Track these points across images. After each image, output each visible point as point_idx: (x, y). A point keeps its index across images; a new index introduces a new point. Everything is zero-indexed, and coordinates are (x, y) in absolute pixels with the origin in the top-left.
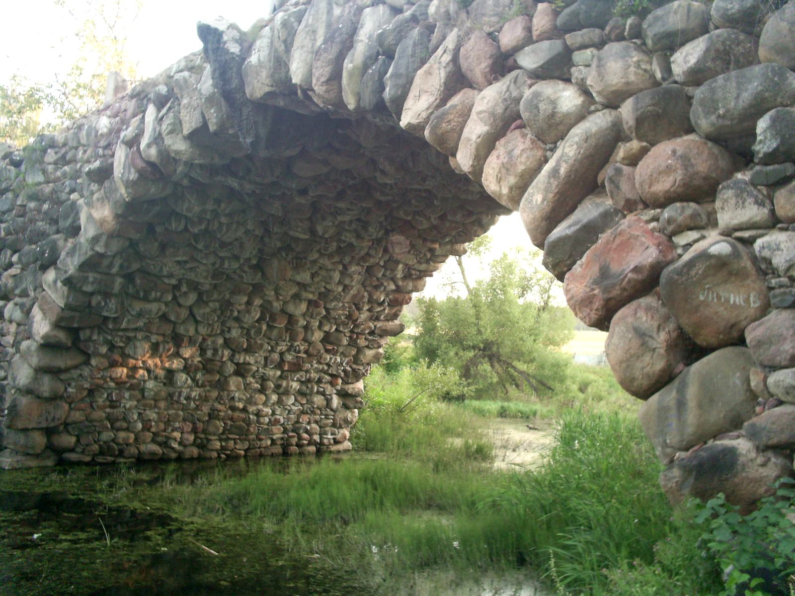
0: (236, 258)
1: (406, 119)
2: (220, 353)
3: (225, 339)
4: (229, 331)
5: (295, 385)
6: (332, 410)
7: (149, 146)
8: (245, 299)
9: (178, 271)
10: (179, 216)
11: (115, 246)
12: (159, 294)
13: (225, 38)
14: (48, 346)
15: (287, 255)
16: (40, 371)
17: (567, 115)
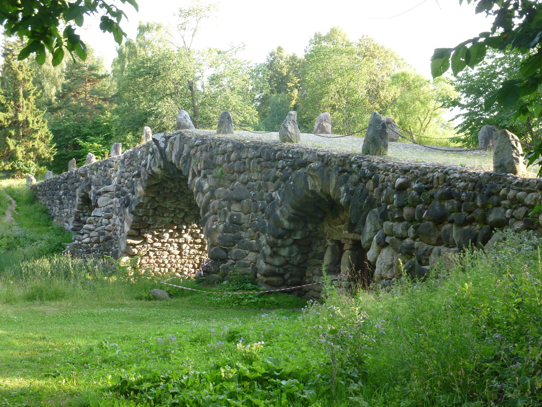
7: (148, 169)
9: (172, 205)
10: (167, 188)
11: (146, 200)
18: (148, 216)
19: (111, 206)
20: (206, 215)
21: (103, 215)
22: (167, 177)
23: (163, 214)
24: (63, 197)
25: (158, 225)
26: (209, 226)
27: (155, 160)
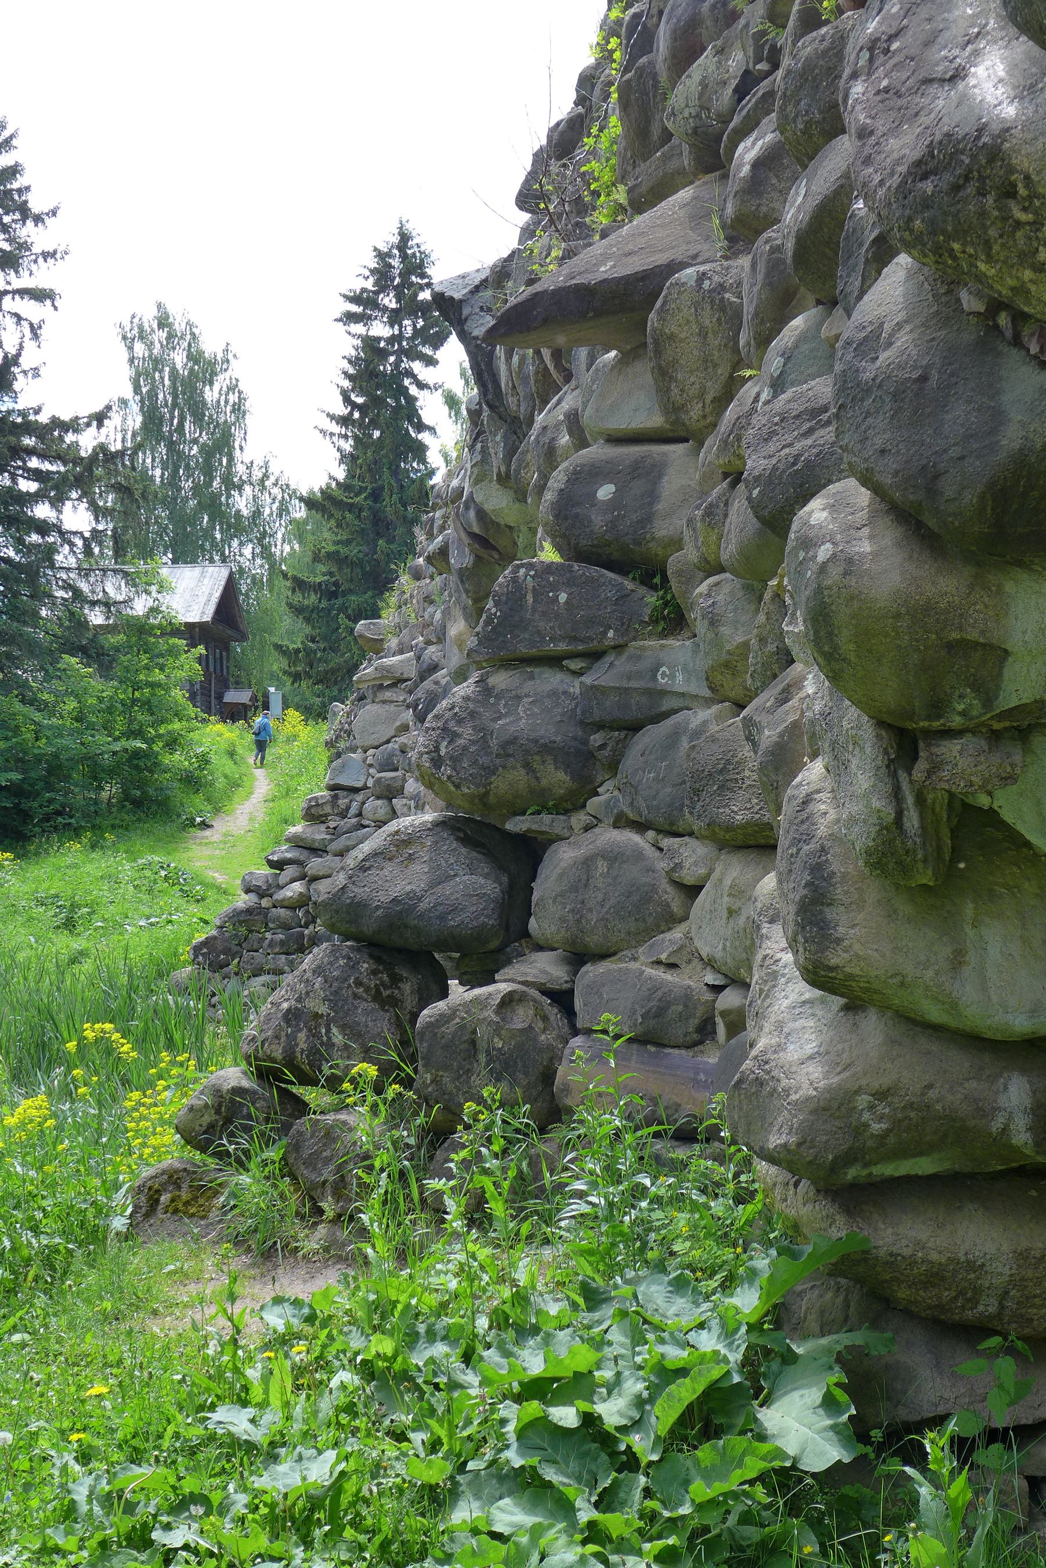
13: (466, 312)
19: (402, 740)
21: (370, 783)
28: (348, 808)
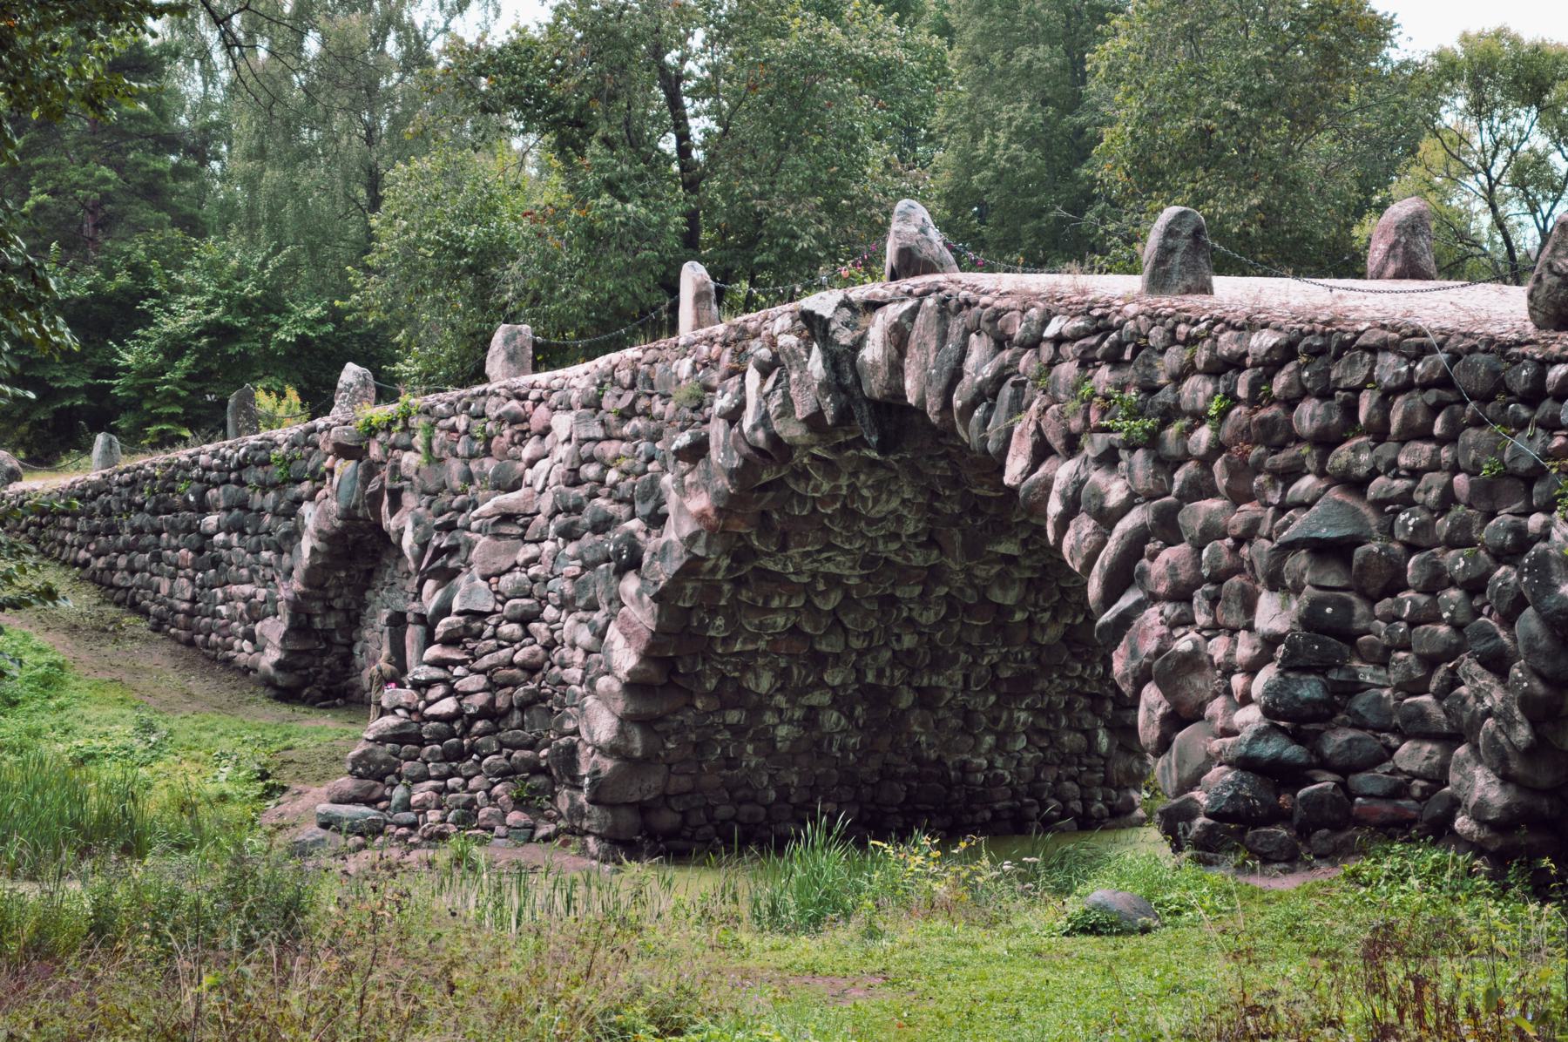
0: (895, 536)
1: (1008, 479)
2: (888, 673)
3: (894, 652)
4: (899, 638)
5: (1023, 716)
6: (1100, 756)
7: (754, 428)
8: (918, 590)
10: (802, 499)
12: (784, 599)
13: (833, 326)
14: (635, 686)
15: (974, 521)
16: (624, 720)
17: (1112, 510)
18: (714, 611)
20: (1126, 601)
22: (814, 457)
23: (767, 600)
24: (220, 537)
25: (744, 642)
26: (1150, 646)
27: (786, 395)
28: (482, 631)
